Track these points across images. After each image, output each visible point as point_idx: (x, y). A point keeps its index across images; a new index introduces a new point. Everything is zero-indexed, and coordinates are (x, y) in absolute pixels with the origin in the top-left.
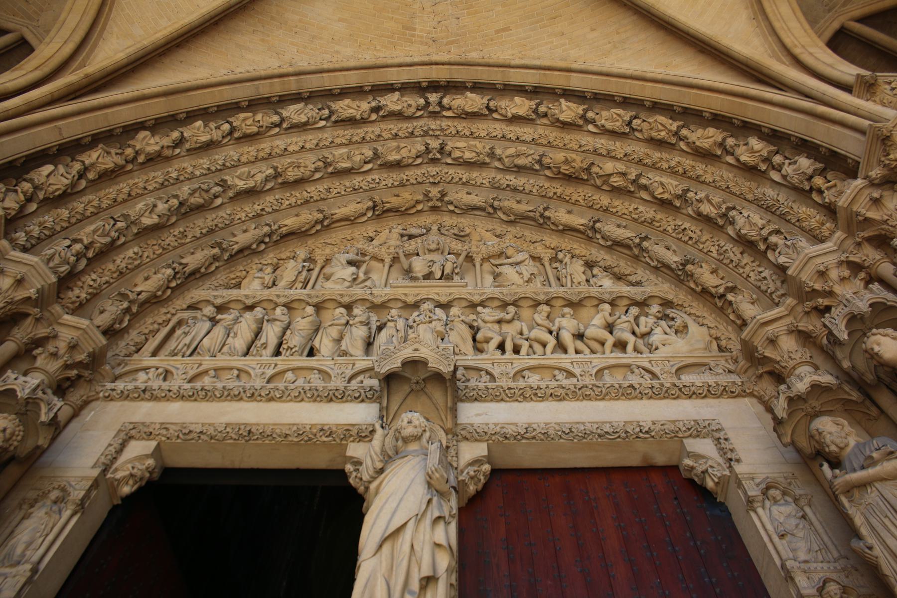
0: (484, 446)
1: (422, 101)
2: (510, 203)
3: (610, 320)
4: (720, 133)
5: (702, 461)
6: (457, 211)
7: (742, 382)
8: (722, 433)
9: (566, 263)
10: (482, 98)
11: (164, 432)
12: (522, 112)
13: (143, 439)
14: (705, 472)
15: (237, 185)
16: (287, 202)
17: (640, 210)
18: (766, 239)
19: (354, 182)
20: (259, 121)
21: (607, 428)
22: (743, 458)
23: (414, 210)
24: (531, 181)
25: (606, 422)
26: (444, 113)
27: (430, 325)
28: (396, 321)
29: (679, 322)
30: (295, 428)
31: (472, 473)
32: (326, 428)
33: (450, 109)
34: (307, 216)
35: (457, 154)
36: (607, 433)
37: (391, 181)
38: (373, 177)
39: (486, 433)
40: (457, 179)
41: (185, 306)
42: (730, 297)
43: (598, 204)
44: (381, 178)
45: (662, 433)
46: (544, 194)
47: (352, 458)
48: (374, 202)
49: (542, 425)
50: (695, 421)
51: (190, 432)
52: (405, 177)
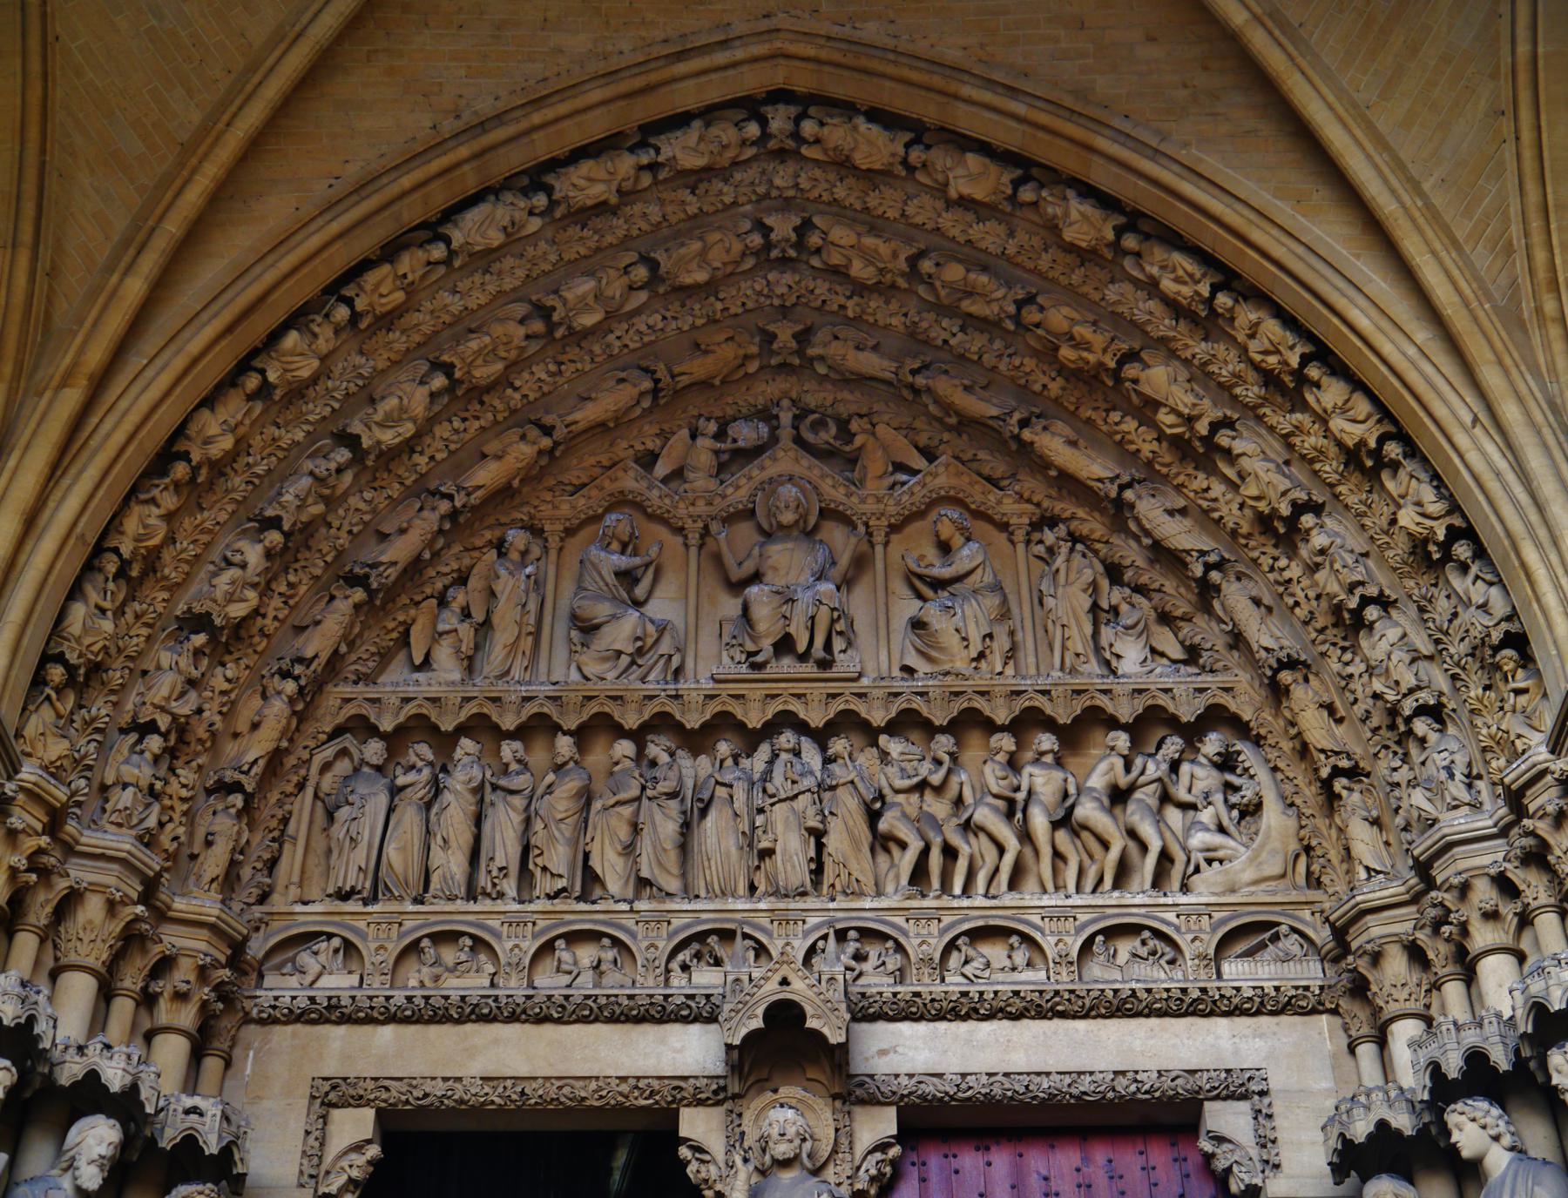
0: (892, 1112)
1: (753, 129)
2: (948, 388)
3: (1123, 781)
4: (1379, 421)
5: (1226, 1147)
6: (832, 375)
7: (1322, 988)
8: (1266, 1101)
9: (1058, 571)
10: (892, 140)
11: (384, 1096)
12: (979, 192)
13: (350, 1105)
14: (1229, 1170)
15: (379, 442)
16: (477, 424)
17: (1212, 494)
18: (1408, 720)
19: (611, 338)
20: (405, 276)
21: (1085, 1084)
22: (1284, 1165)
23: (741, 373)
24: (998, 344)
25: (1084, 1073)
26: (804, 150)
27: (795, 804)
28: (731, 786)
29: (1248, 794)
30: (593, 1085)
31: (873, 1172)
32: (641, 1085)
33: (818, 141)
34: (523, 451)
35: (836, 259)
36: (1085, 1093)
37: (690, 320)
38: (651, 322)
39: (894, 1093)
40: (835, 307)
41: (323, 737)
42: (1339, 784)
43: (1132, 442)
44: (668, 315)
45: (1171, 1093)
46: (1023, 382)
47: (687, 1140)
48: (656, 381)
49: (984, 1079)
50: (1228, 1071)
51: (426, 1095)
52: (719, 306)
